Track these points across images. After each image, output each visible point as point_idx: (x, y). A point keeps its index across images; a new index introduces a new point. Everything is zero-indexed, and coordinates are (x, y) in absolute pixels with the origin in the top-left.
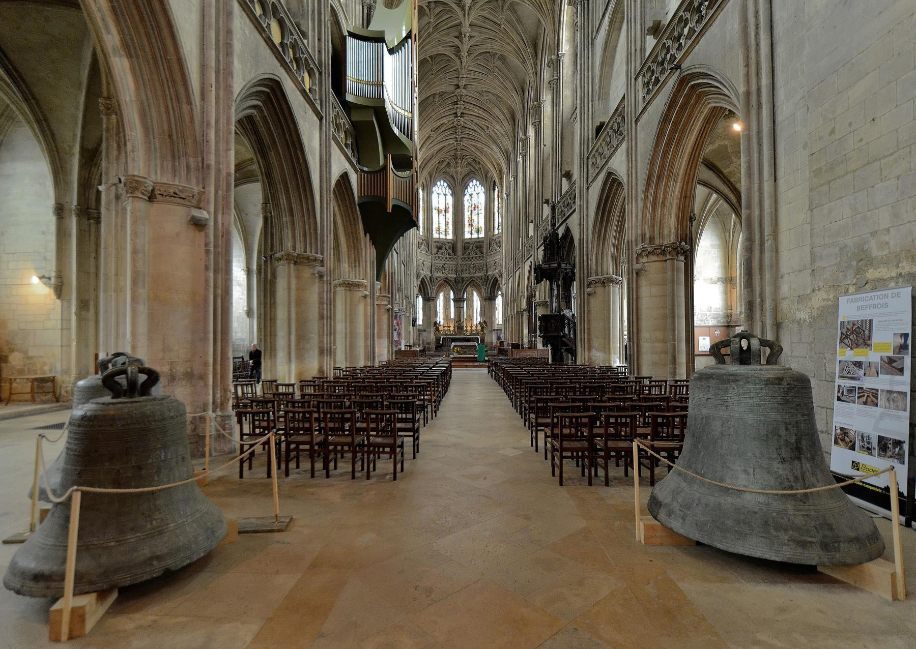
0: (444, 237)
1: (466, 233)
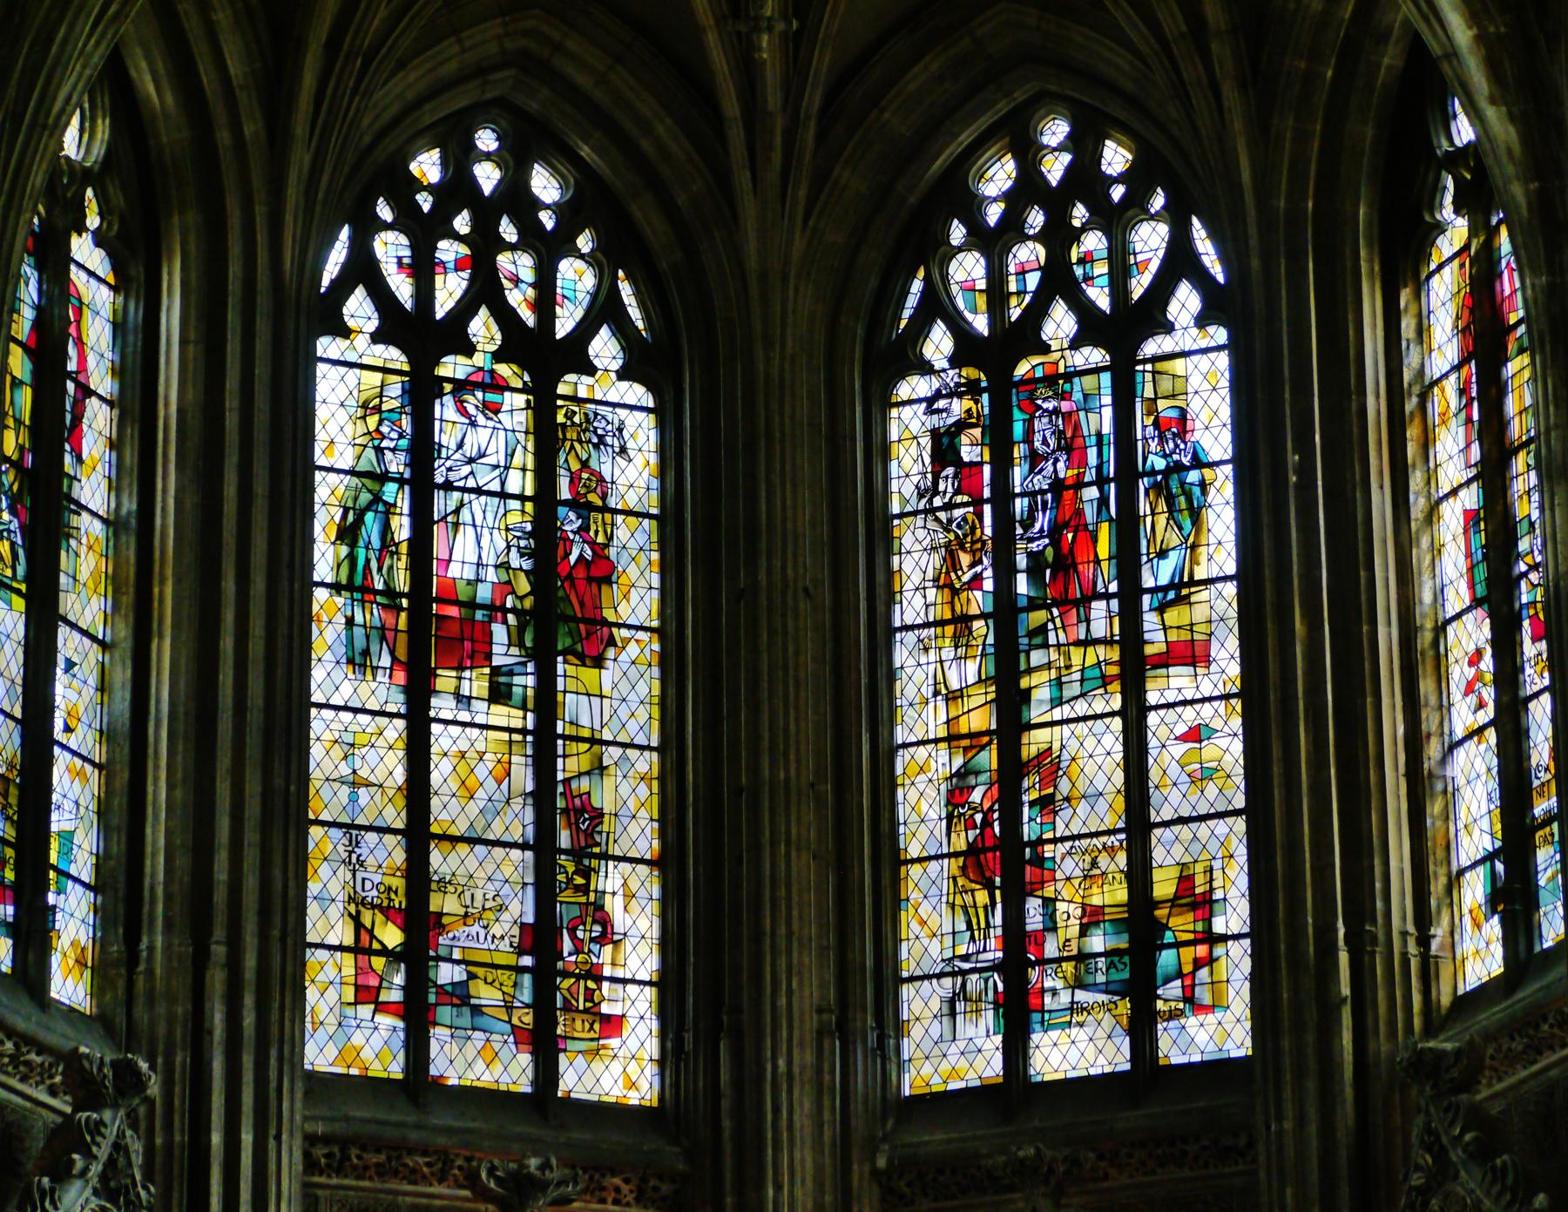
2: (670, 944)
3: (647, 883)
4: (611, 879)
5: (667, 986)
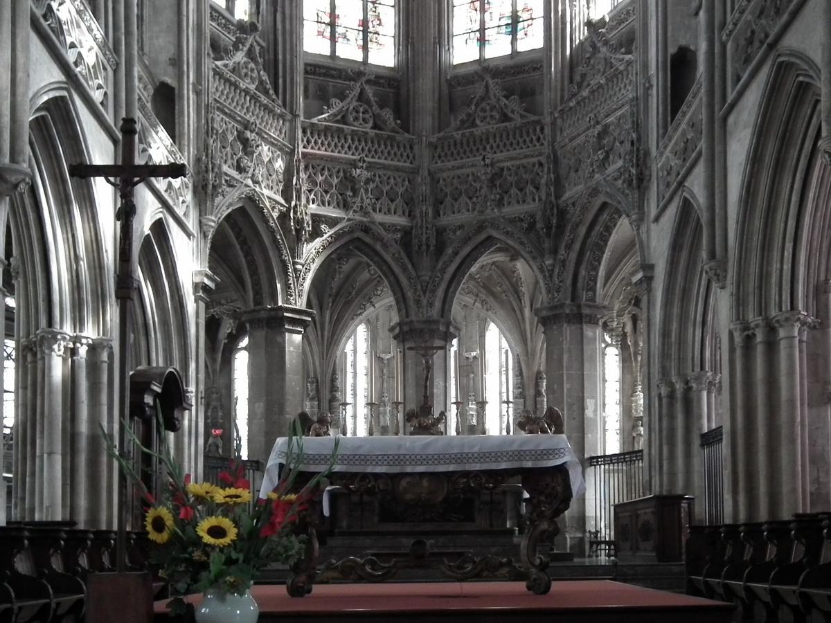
0: (359, 57)
1: (457, 42)
2: (398, 26)
3: (392, 12)
4: (380, 9)
5: (397, 38)
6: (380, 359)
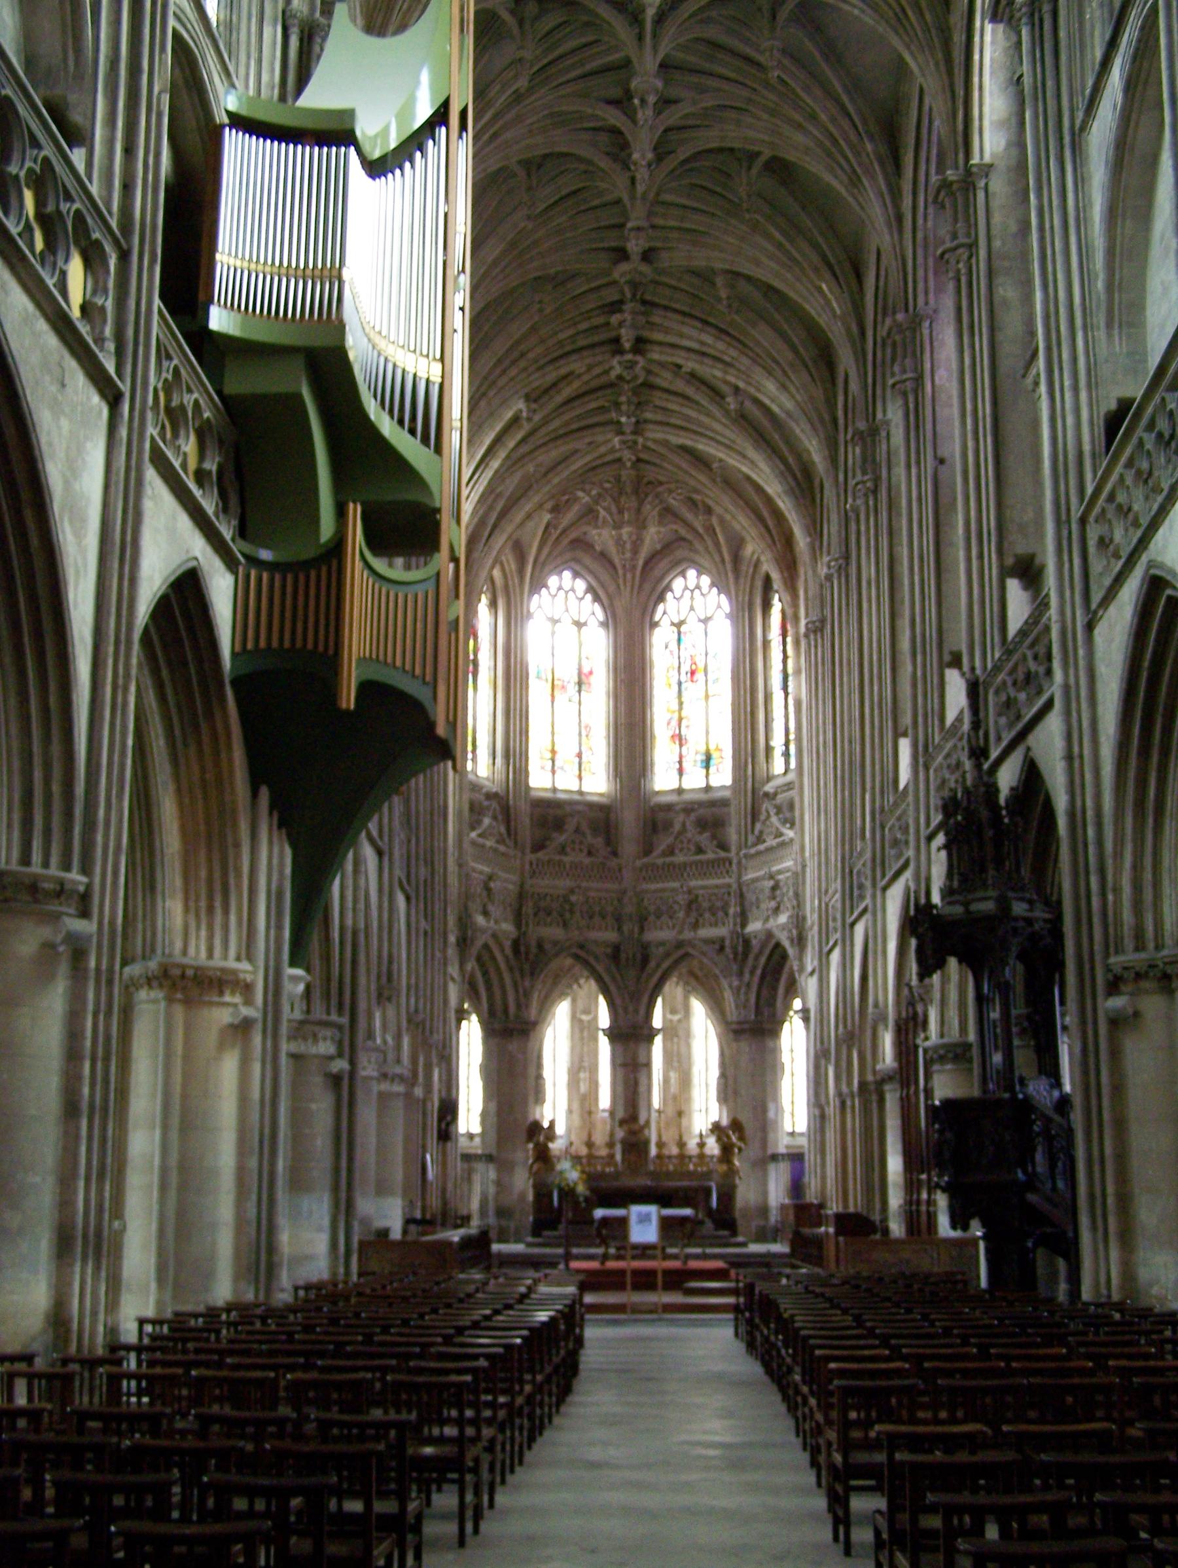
6: (581, 1021)
